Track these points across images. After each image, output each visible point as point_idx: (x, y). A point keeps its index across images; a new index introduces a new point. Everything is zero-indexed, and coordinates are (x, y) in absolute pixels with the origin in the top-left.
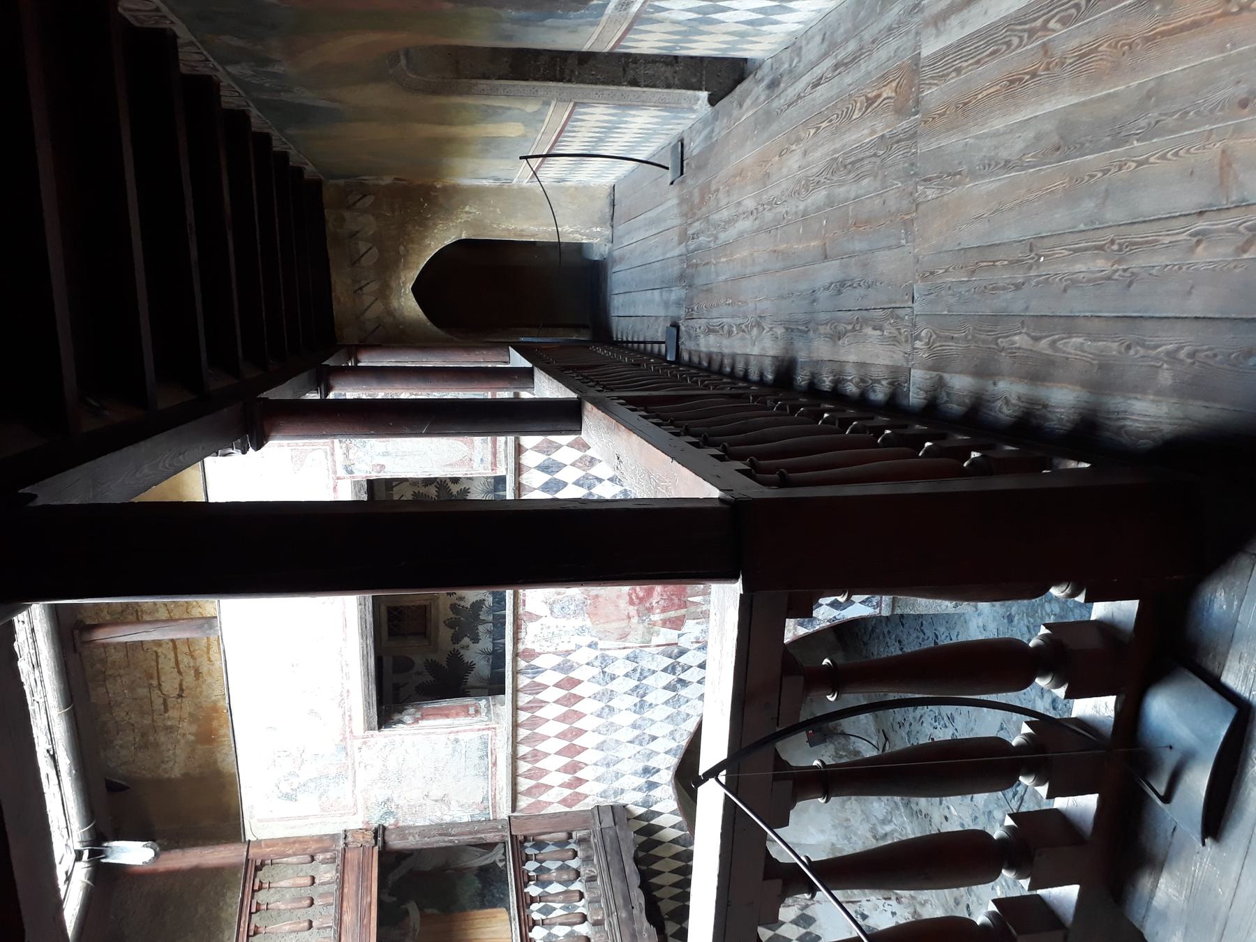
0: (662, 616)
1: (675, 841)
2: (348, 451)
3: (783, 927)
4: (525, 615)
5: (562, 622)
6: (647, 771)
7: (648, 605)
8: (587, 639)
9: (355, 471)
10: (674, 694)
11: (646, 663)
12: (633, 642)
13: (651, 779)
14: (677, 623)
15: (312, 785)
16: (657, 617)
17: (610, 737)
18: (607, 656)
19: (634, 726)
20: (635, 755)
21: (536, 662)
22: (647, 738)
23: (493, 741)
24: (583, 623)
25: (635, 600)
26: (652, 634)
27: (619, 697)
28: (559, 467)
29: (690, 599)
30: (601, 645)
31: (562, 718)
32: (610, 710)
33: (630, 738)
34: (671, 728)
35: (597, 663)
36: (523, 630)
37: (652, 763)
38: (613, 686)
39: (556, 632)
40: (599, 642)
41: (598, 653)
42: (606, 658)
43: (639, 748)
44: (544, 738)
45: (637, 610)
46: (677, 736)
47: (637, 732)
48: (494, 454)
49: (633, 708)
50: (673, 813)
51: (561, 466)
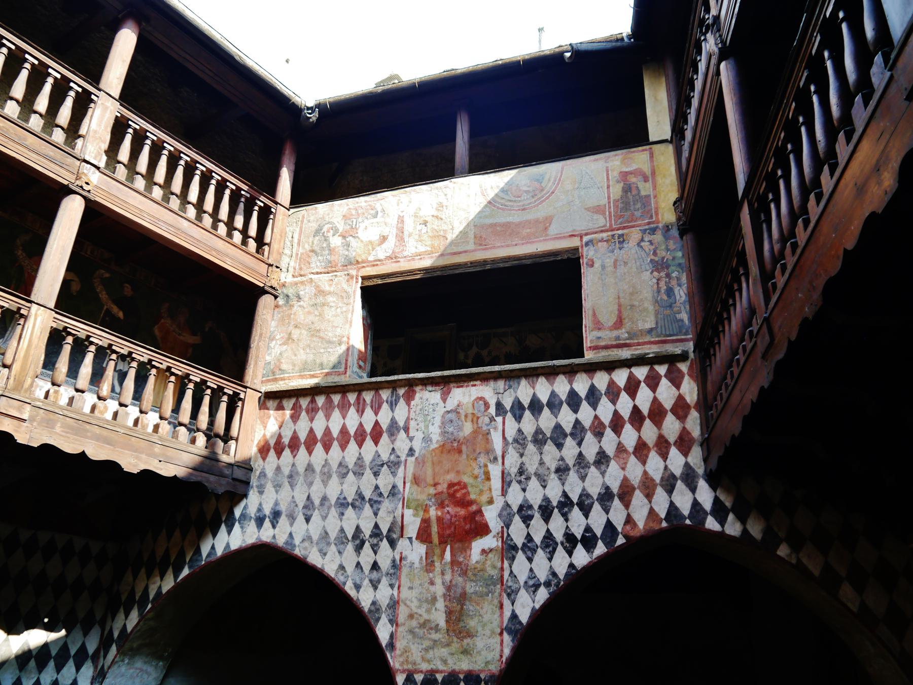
0: (433, 519)
1: (198, 551)
2: (605, 241)
3: (73, 669)
4: (448, 389)
5: (438, 421)
6: (276, 515)
7: (446, 502)
8: (417, 445)
9: (588, 248)
10: (350, 537)
11: (386, 505)
12: (409, 491)
13: (267, 520)
14: (424, 535)
15: (325, 245)
16: (433, 513)
17: (318, 476)
18: (399, 467)
19: (324, 499)
20: (295, 502)
21: (402, 402)
22: (309, 513)
23: (334, 374)
24: (434, 440)
25: (451, 491)
27: (356, 481)
28: (593, 404)
29: (448, 548)
30: (411, 460)
31: (344, 431)
32: (345, 474)
33: (313, 496)
34: (315, 537)
35: (392, 457)
36: (434, 388)
37: (283, 521)
38: (368, 473)
39: (429, 418)
40: (413, 459)
41: (403, 458)
42: (397, 467)
43: (301, 505)
44: (328, 417)
45: (442, 492)
46: (306, 544)
47: (317, 502)
48: (606, 347)
49: (342, 497)
50: (228, 545)
51: (594, 404)
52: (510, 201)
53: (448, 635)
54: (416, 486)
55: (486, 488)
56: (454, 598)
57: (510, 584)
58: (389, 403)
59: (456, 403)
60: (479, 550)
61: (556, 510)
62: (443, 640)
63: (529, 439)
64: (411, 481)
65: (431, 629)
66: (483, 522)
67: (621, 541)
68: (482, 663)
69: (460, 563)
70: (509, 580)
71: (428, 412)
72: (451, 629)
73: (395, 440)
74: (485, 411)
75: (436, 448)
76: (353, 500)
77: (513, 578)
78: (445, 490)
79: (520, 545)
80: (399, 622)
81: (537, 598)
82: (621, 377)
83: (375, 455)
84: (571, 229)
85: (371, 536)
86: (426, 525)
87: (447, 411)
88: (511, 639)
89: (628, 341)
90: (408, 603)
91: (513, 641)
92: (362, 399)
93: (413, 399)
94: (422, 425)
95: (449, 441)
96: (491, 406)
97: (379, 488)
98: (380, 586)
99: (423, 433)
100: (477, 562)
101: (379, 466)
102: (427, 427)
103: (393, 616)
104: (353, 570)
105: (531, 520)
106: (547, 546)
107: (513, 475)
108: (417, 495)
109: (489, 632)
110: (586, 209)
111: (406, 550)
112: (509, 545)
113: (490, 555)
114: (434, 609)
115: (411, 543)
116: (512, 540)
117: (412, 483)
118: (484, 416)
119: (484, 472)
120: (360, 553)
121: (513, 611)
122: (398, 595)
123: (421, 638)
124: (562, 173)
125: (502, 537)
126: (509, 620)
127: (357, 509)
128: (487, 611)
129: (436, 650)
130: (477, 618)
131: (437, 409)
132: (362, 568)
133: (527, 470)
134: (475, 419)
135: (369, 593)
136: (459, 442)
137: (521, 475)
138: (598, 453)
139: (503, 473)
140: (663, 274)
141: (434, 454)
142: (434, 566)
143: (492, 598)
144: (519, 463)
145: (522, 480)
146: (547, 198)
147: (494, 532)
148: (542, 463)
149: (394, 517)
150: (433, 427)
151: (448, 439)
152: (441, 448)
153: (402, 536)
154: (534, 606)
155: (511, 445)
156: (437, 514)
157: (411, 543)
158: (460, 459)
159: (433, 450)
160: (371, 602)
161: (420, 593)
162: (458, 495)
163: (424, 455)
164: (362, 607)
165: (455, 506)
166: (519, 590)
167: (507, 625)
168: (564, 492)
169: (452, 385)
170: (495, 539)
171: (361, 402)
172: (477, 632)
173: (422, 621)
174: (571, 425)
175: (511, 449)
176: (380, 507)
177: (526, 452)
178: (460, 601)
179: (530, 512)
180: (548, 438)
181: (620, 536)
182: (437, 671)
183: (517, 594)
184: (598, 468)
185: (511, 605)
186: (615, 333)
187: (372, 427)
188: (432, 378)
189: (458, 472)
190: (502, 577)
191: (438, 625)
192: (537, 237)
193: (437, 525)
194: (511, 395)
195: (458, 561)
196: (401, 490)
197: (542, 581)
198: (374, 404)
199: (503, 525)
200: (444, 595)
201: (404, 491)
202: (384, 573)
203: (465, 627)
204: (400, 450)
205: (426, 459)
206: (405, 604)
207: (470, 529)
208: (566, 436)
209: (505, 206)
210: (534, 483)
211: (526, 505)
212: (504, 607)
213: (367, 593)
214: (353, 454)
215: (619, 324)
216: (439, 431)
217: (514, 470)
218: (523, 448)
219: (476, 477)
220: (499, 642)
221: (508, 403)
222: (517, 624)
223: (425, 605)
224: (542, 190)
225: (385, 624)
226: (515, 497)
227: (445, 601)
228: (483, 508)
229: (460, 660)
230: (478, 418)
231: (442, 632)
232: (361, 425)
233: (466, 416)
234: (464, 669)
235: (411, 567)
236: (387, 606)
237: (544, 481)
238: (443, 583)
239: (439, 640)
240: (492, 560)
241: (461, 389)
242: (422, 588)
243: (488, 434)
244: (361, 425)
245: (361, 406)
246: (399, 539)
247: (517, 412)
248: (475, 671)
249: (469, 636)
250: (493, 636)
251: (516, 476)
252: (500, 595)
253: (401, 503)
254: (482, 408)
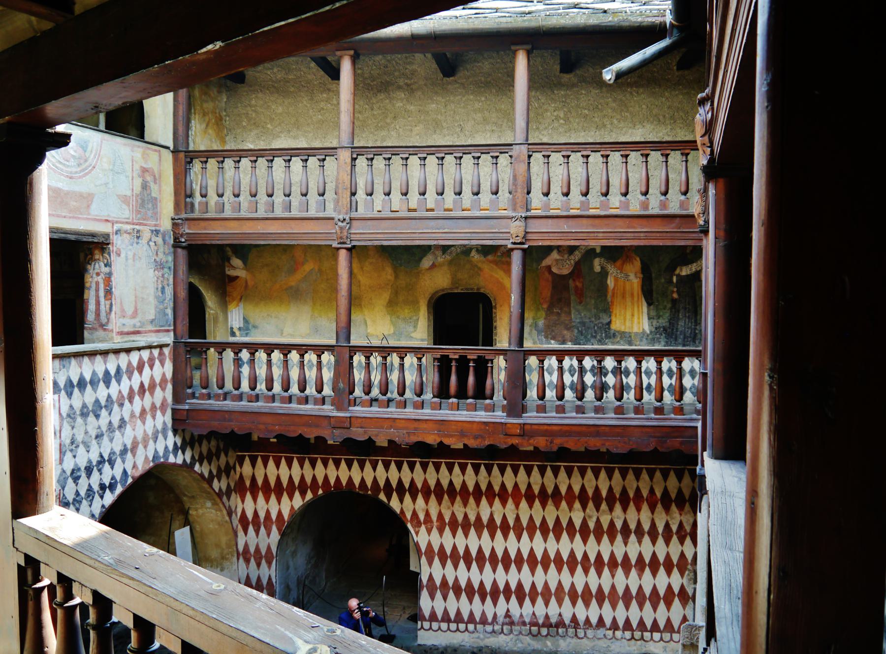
48: (128, 333)
52: (60, 163)
61: (95, 468)
63: (78, 413)
67: (130, 480)
82: (134, 357)
84: (106, 214)
89: (140, 329)
106: (89, 496)
110: (117, 196)
124: (101, 147)
125: (59, 498)
138: (120, 420)
139: (60, 445)
140: (160, 274)
146: (90, 172)
148: (86, 433)
168: (101, 453)
174: (105, 399)
175: (65, 423)
179: (79, 474)
181: (130, 478)
184: (120, 432)
186: (133, 322)
192: (81, 214)
208: (101, 408)
209: (56, 167)
210: (81, 450)
215: (135, 314)
217: (68, 441)
221: (62, 383)
224: (86, 161)
226: (68, 465)
247: (69, 390)
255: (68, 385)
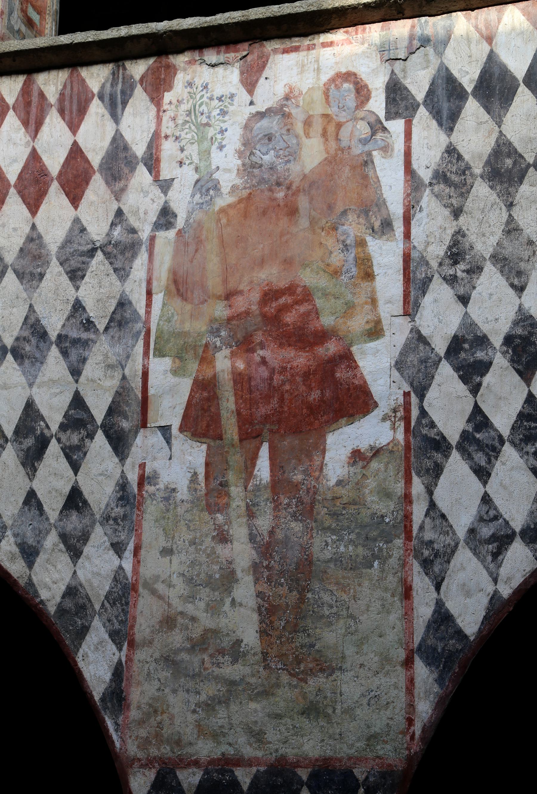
7: (259, 337)
18: (134, 256)
24: (225, 188)
25: (272, 308)
26: (180, 358)
27: (24, 295)
29: (265, 451)
36: (222, 58)
39: (211, 132)
40: (171, 234)
41: (145, 234)
42: (128, 255)
45: (247, 313)
53: (267, 667)
54: (178, 302)
55: (361, 299)
56: (282, 573)
57: (428, 535)
58: (107, 99)
59: (280, 91)
60: (344, 454)
62: (253, 680)
63: (478, 171)
64: (167, 288)
65: (222, 652)
66: (357, 382)
68: (359, 740)
69: (297, 486)
70: (427, 527)
71: (209, 117)
72: (273, 652)
73: (123, 190)
74: (357, 108)
75: (229, 206)
76: (17, 339)
77: (438, 522)
78: (254, 308)
79: (453, 437)
80: (138, 637)
81: (504, 571)
83: (71, 230)
85: (63, 427)
86: (205, 394)
87: (258, 113)
88: (435, 675)
90: (160, 587)
91: (440, 681)
92: (35, 94)
93: (169, 88)
94: (193, 151)
95: (263, 187)
96: (373, 94)
97: (84, 309)
98: (88, 550)
99: (197, 169)
100: (340, 483)
101: (82, 254)
102: (206, 154)
103: (121, 622)
104: (16, 512)
105: (483, 375)
107: (434, 264)
108: (183, 322)
109: (376, 659)
111: (155, 459)
112: (426, 439)
113: (374, 465)
114: (228, 601)
115: (168, 440)
116: (432, 425)
117: (168, 293)
118: (355, 119)
119: (356, 259)
120: (35, 470)
121: (440, 604)
122: (135, 571)
123: (194, 676)
125: (407, 419)
126: (428, 627)
127: (27, 361)
128: (368, 606)
129: (234, 707)
130: (342, 622)
131: (231, 108)
132: (40, 506)
133: (472, 248)
134: (331, 129)
135: (59, 567)
136: (288, 188)
137: (456, 263)
139: (407, 258)
141: (224, 221)
142: (228, 494)
143: (383, 571)
144: (450, 232)
145: (459, 274)
147: (384, 408)
149: (124, 378)
150: (222, 154)
151: (262, 181)
152: (242, 205)
153: (144, 425)
154: (496, 592)
155: (428, 191)
156: (233, 366)
157: (168, 440)
158: (294, 230)
159: (223, 210)
160: (63, 588)
161: (193, 564)
162: (290, 318)
163: (200, 225)
164: (42, 602)
165: (281, 346)
166: (453, 552)
167: (423, 640)
169: (270, 46)
170: (388, 423)
171: (35, 99)
172: (343, 657)
173: (197, 633)
176: (87, 353)
177: (469, 204)
178: (298, 580)
179: (480, 355)
180: (529, 166)
182: (239, 762)
183: (449, 562)
185: (432, 588)
187: (62, 160)
188: (220, 28)
189: (288, 263)
190: (408, 517)
191: (239, 642)
193: (236, 394)
194: (428, 61)
195: (290, 482)
196: (142, 311)
197: (517, 525)
198: (67, 103)
199: (407, 388)
200: (255, 567)
201: (148, 313)
202: (98, 516)
203: (312, 646)
204: (136, 213)
205: (204, 232)
206: (154, 592)
207: (322, 400)
211: (470, 337)
212: (414, 593)
213: (55, 566)
214: (15, 229)
216: (236, 162)
218: (462, 195)
219: (336, 273)
220: (402, 682)
222: (452, 638)
223: (205, 593)
225: (101, 643)
227: (257, 581)
228: (354, 349)
229: (298, 731)
230: (339, 126)
231: (251, 659)
232: (34, 156)
233: (308, 123)
234: (311, 755)
235: (167, 499)
236: (106, 597)
237: (519, 274)
238: (252, 538)
239: (242, 680)
240: (381, 476)
241: (293, 55)
242: (197, 551)
243: (366, 163)
244: (34, 156)
245: (34, 110)
246: (136, 433)
248: (340, 760)
249: (322, 670)
250: (387, 668)
251: (441, 264)
252: (404, 564)
253: (141, 343)
254: (351, 101)
255: (441, 92)
